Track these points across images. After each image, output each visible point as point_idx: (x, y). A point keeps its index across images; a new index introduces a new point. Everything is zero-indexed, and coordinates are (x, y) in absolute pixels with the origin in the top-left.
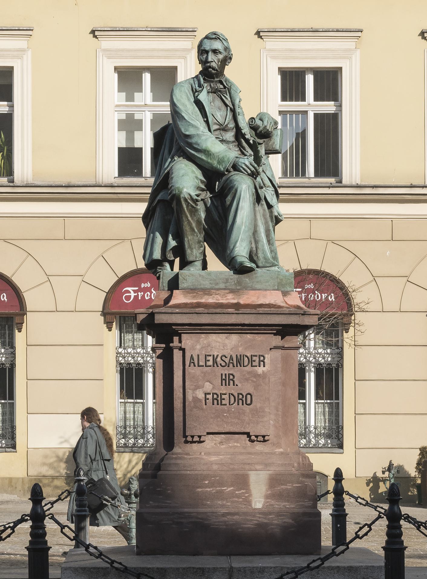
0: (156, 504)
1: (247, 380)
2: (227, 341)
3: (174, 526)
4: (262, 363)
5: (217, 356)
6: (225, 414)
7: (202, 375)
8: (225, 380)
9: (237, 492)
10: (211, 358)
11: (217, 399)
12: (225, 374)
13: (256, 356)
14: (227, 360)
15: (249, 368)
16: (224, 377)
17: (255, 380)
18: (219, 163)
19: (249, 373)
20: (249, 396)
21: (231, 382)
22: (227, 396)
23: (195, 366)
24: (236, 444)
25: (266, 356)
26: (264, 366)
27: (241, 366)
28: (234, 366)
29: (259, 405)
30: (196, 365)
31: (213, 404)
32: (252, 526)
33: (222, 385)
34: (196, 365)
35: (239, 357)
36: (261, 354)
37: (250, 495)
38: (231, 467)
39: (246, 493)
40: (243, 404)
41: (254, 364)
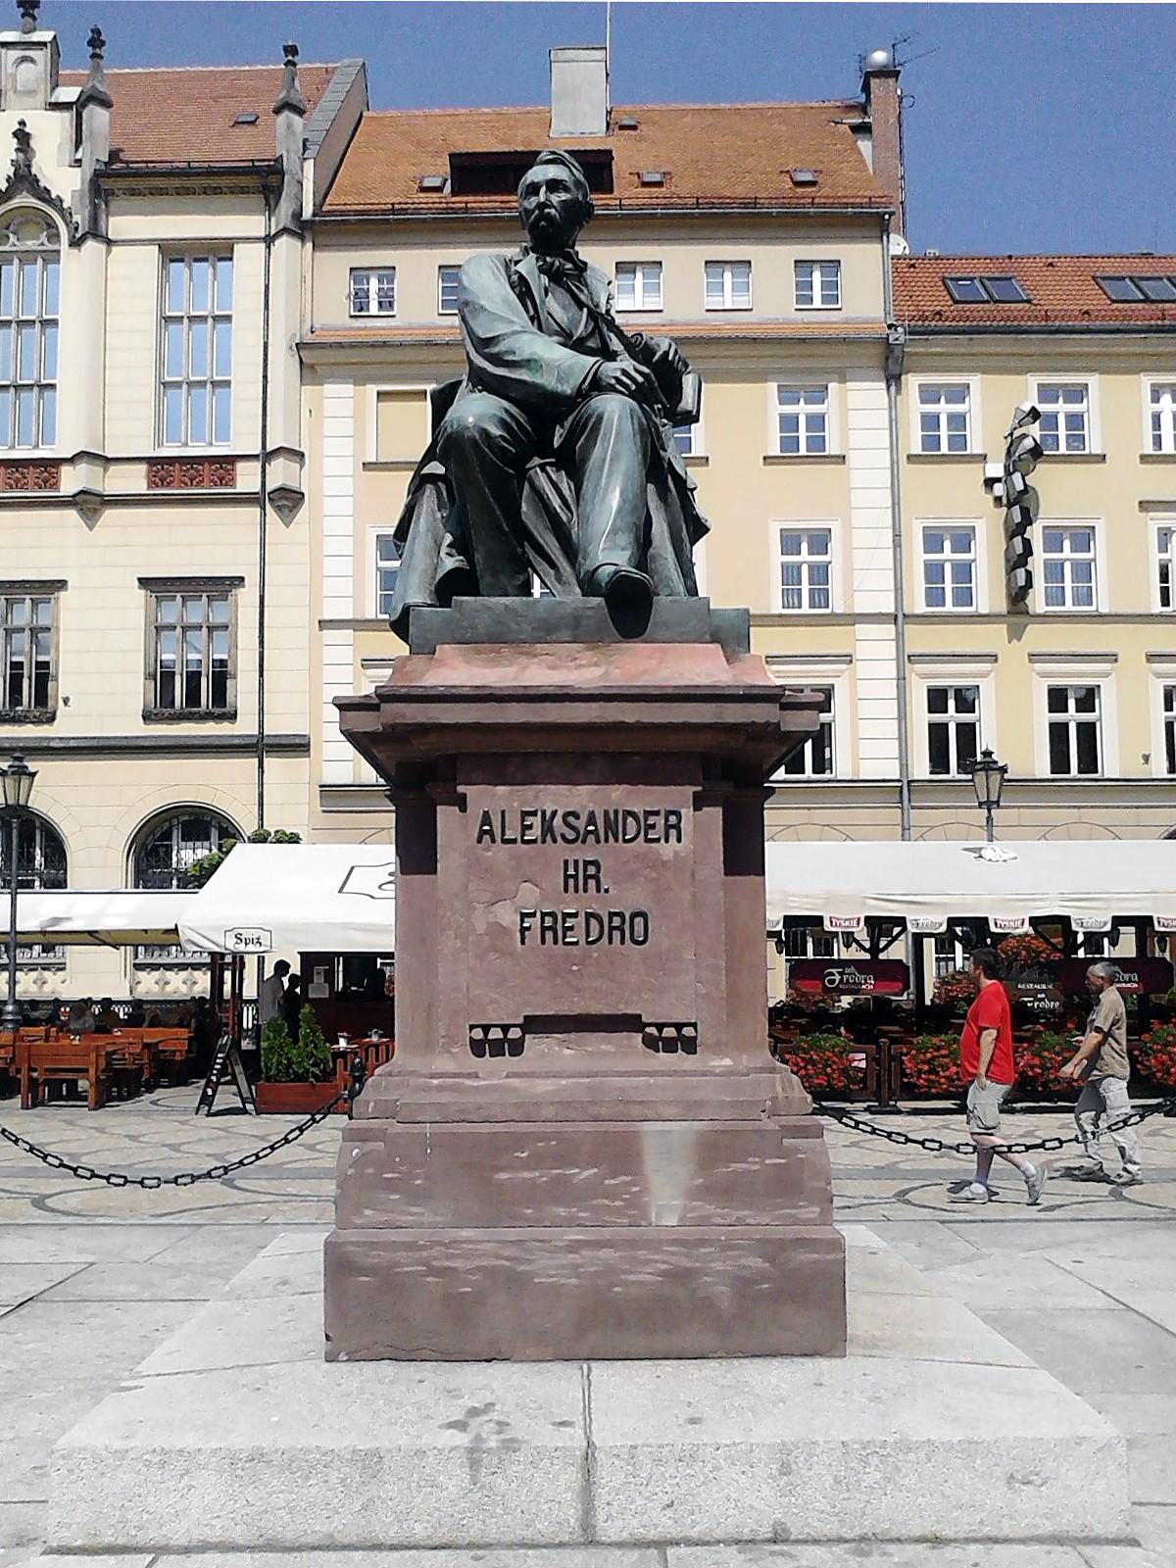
1: (632, 875)
4: (673, 833)
5: (554, 813)
6: (575, 968)
7: (513, 863)
8: (575, 877)
10: (537, 821)
11: (554, 927)
12: (576, 862)
13: (657, 813)
14: (580, 824)
16: (571, 872)
18: (560, 380)
20: (639, 921)
21: (592, 883)
22: (582, 918)
23: (493, 841)
25: (683, 811)
26: (679, 840)
27: (616, 840)
28: (598, 841)
29: (665, 943)
30: (498, 839)
31: (543, 942)
33: (566, 890)
34: (498, 839)
35: (612, 816)
38: (593, 1111)
39: (632, 1184)
40: (623, 942)
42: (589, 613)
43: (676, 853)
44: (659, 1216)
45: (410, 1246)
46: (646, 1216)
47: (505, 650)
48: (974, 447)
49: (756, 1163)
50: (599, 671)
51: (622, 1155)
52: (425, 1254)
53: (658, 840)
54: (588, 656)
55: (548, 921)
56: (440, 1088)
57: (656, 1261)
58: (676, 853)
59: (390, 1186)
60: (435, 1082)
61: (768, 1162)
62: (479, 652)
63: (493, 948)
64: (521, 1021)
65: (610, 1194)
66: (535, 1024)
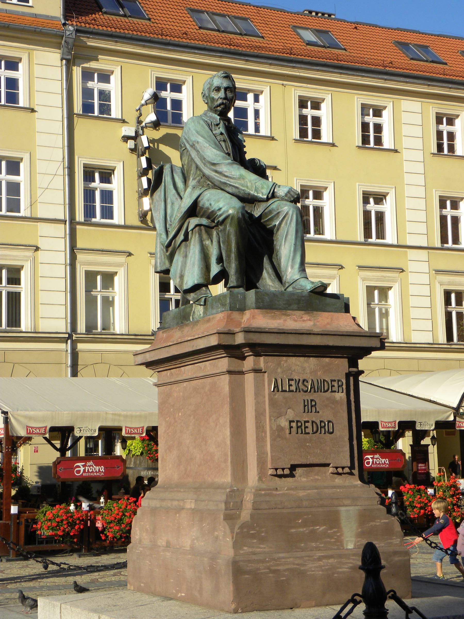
0: (250, 550)
2: (306, 365)
3: (271, 575)
6: (308, 444)
9: (329, 532)
11: (300, 427)
15: (328, 394)
17: (333, 406)
19: (328, 399)
20: (331, 424)
24: (316, 477)
28: (315, 392)
30: (280, 390)
31: (297, 433)
32: (350, 570)
33: (304, 412)
36: (338, 379)
37: (342, 535)
38: (321, 502)
41: (334, 389)
42: (303, 298)
43: (341, 397)
44: (347, 545)
45: (263, 561)
46: (342, 545)
47: (277, 313)
48: (115, 113)
49: (378, 522)
51: (333, 521)
52: (268, 564)
53: (335, 392)
54: (306, 317)
55: (299, 424)
56: (265, 495)
57: (349, 563)
58: (341, 397)
59: (253, 536)
60: (263, 492)
61: (382, 521)
62: (268, 313)
63: (279, 436)
64: (289, 466)
65: (330, 537)
66: (293, 468)
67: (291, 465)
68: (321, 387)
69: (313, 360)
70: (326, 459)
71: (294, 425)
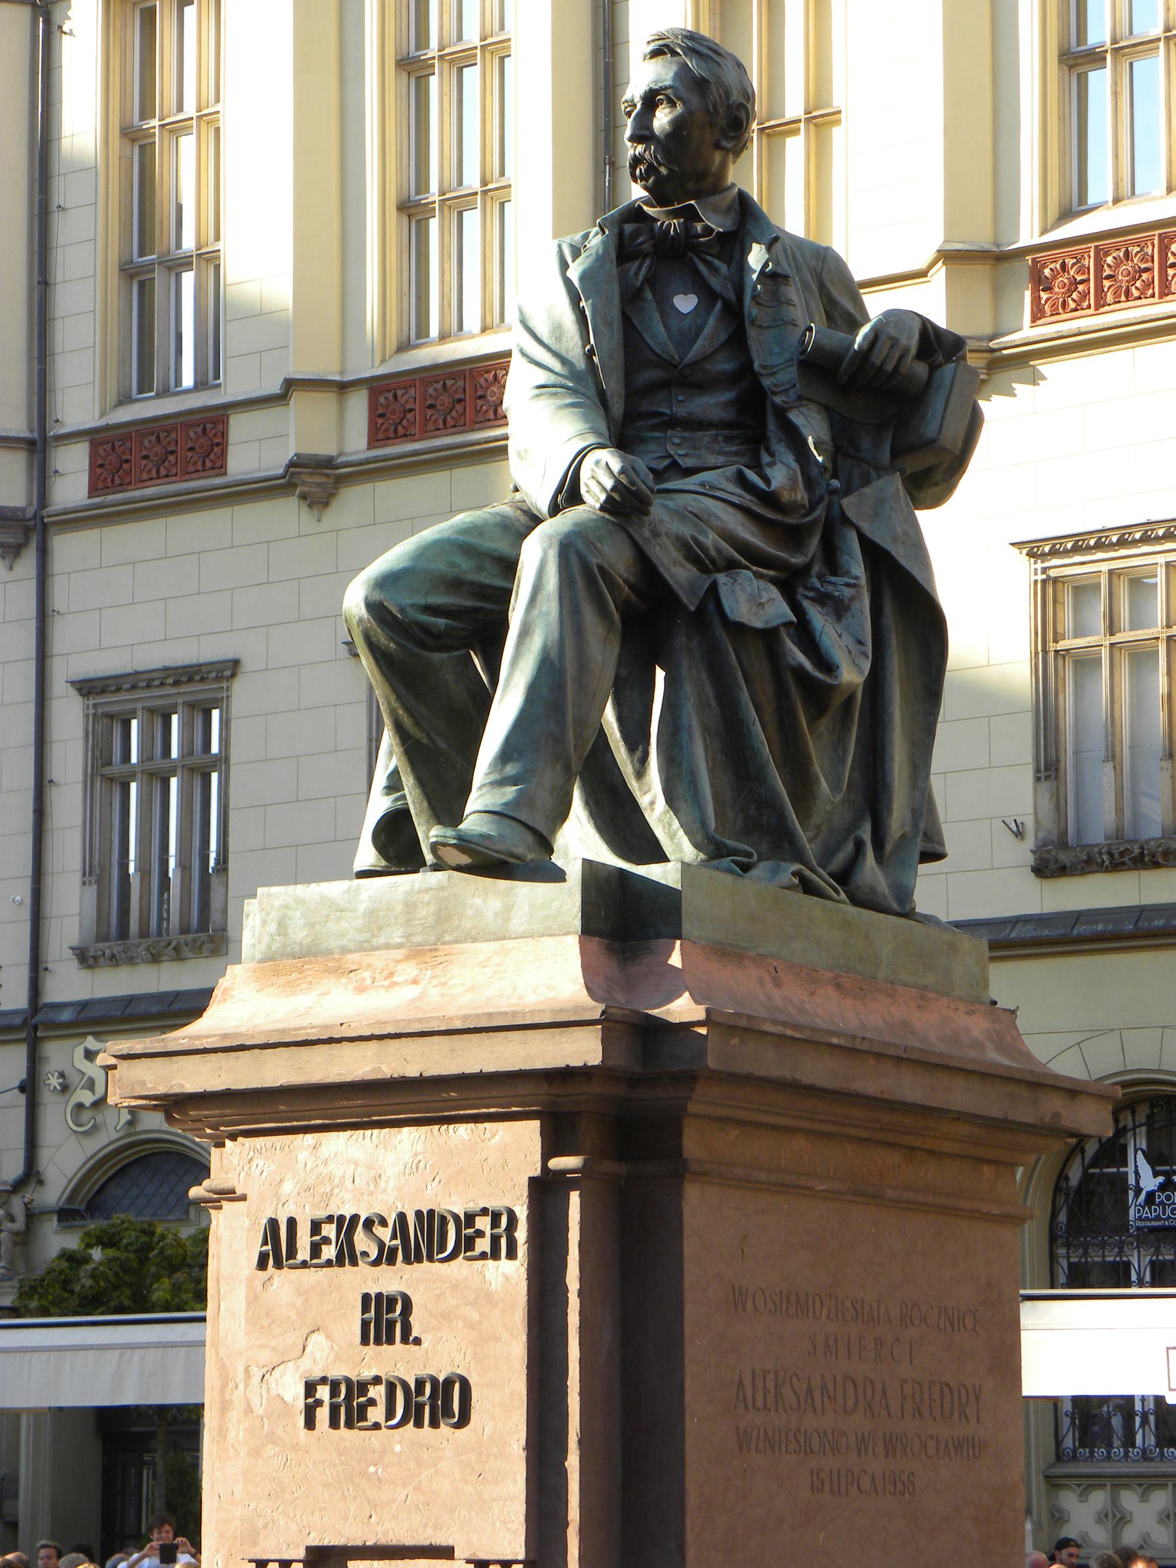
1: (446, 1317)
6: (372, 1469)
7: (299, 1302)
11: (348, 1404)
19: (455, 1286)
43: (507, 1278)
50: (412, 992)
58: (507, 1278)
64: (301, 1554)
67: (309, 1549)
68: (426, 1236)
69: (409, 1139)
70: (435, 1528)
71: (323, 1392)
